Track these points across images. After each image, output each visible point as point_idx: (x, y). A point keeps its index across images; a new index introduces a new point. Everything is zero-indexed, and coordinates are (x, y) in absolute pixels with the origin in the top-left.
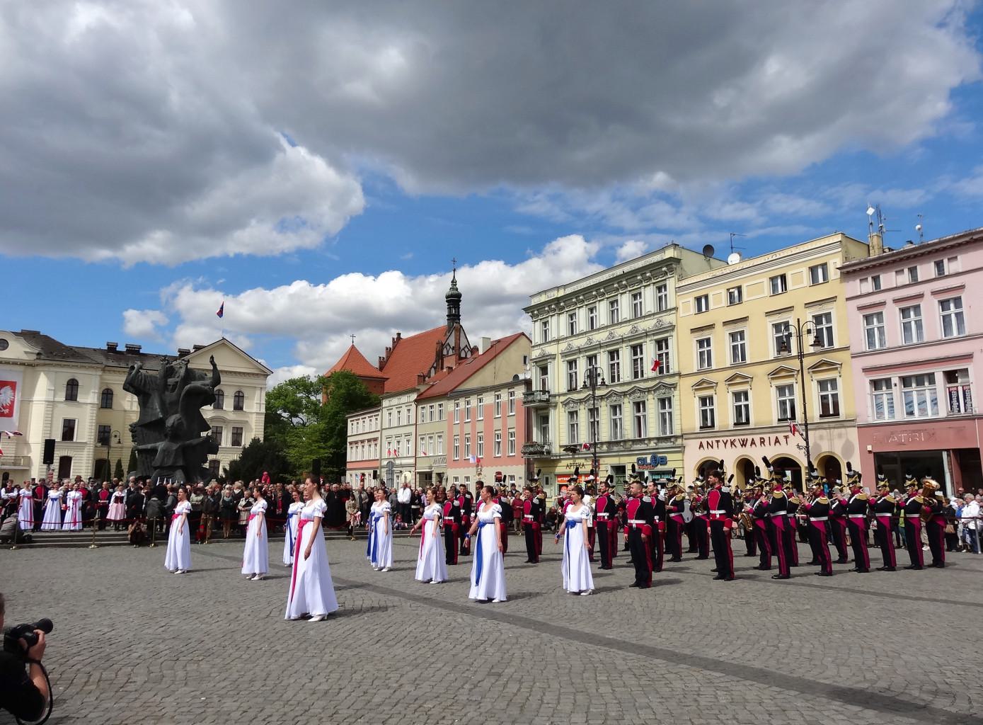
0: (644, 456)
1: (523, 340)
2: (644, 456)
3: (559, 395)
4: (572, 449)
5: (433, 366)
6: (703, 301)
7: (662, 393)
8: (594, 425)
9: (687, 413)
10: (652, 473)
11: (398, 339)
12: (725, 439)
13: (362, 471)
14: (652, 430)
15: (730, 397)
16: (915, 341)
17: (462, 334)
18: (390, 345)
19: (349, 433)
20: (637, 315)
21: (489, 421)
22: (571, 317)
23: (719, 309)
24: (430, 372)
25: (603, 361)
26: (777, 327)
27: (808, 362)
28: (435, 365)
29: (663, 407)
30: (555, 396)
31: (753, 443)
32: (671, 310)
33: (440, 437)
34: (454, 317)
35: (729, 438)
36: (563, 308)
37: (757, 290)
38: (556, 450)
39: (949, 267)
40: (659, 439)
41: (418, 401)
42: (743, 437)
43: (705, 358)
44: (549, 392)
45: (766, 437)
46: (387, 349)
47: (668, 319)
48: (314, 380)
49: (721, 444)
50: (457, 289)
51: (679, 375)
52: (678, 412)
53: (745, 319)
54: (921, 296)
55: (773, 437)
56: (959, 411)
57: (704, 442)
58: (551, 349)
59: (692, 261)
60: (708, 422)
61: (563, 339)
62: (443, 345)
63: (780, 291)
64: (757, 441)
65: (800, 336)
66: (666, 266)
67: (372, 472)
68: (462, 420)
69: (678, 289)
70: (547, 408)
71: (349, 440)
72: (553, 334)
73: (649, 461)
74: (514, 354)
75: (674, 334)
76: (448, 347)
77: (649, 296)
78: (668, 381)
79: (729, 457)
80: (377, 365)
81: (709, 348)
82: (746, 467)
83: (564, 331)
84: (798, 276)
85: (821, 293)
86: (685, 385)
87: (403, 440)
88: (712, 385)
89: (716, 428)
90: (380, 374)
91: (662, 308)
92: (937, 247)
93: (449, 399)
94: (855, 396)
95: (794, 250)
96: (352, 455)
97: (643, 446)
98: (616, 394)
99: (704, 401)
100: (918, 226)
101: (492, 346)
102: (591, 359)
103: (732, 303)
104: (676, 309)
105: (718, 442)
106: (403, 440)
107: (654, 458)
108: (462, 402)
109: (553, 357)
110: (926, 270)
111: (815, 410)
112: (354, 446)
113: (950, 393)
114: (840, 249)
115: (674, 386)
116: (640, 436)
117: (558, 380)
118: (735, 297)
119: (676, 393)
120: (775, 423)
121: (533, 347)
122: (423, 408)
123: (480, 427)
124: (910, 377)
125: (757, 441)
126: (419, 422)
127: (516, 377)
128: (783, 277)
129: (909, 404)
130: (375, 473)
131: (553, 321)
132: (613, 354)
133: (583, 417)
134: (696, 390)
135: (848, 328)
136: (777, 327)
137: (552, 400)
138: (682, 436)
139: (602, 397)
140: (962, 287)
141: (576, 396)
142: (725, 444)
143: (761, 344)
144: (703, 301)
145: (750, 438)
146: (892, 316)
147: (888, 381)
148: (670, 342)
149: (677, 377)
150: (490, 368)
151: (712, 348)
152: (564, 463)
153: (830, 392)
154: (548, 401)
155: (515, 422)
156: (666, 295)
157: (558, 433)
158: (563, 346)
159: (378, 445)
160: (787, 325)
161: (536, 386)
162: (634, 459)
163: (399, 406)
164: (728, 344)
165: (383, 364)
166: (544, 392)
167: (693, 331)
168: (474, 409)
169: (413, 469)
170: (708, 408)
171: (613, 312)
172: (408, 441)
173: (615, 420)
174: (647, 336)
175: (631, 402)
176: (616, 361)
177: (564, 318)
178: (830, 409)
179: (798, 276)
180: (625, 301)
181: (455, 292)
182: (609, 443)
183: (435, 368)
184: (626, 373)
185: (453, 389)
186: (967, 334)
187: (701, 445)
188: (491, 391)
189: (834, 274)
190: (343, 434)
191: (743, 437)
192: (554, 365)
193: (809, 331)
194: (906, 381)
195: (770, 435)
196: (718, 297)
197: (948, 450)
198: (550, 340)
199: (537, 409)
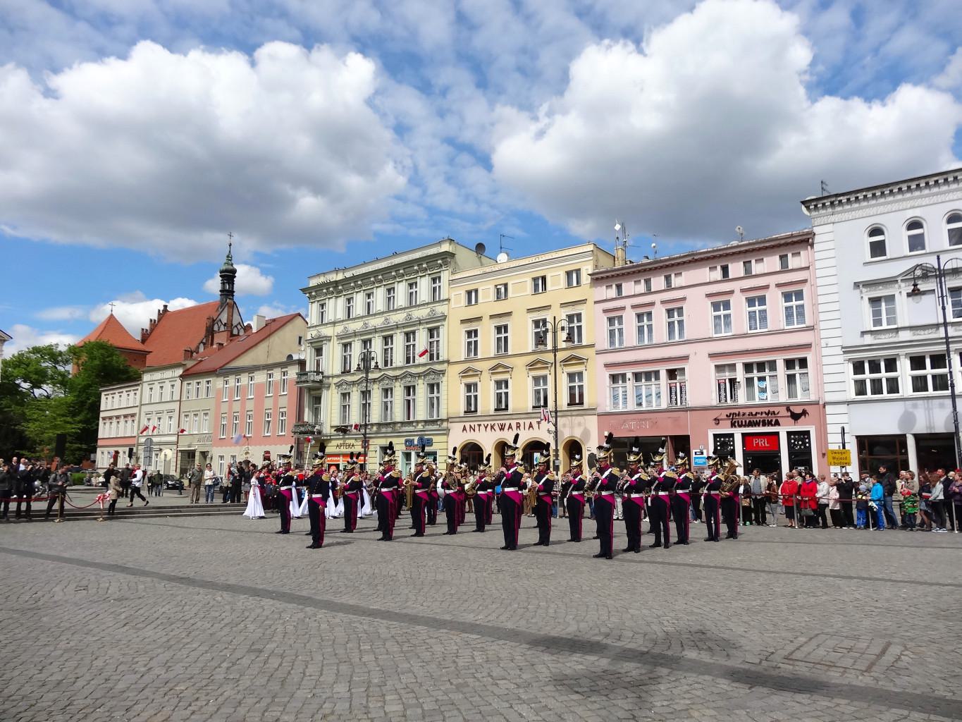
1: (299, 321)
3: (333, 377)
4: (343, 430)
6: (473, 294)
7: (430, 379)
8: (365, 407)
9: (453, 397)
11: (164, 313)
12: (486, 423)
13: (116, 449)
14: (421, 413)
15: (492, 385)
16: (646, 342)
17: (235, 310)
18: (155, 317)
20: (412, 303)
21: (260, 399)
22: (349, 300)
23: (487, 304)
24: (198, 347)
25: (377, 346)
26: (537, 323)
27: (561, 356)
29: (432, 392)
30: (328, 377)
31: (510, 427)
32: (443, 301)
33: (206, 414)
35: (489, 423)
36: (341, 291)
37: (520, 287)
38: (327, 430)
39: (676, 282)
40: (426, 422)
41: (183, 377)
42: (502, 422)
43: (472, 347)
44: (322, 373)
45: (521, 422)
46: (151, 320)
47: (440, 309)
48: (63, 348)
49: (482, 428)
50: (232, 265)
51: (448, 362)
53: (509, 314)
54: (652, 304)
55: (527, 422)
56: (676, 404)
57: (467, 425)
58: (327, 331)
59: (465, 256)
60: (471, 410)
61: (339, 322)
62: (214, 321)
63: (540, 291)
65: (555, 333)
66: (442, 259)
67: (127, 449)
68: (231, 397)
69: (452, 282)
70: (319, 389)
71: (102, 415)
72: (329, 317)
73: (416, 442)
74: (289, 333)
75: (445, 323)
76: (219, 323)
78: (438, 367)
80: (139, 338)
81: (506, 335)
83: (341, 315)
84: (556, 279)
85: (574, 295)
86: (453, 371)
87: (165, 417)
88: (477, 373)
89: (479, 413)
90: (141, 347)
91: (435, 297)
92: (667, 263)
93: (218, 376)
94: (597, 390)
95: (555, 255)
96: (104, 431)
97: (411, 428)
98: (388, 377)
99: (469, 387)
100: (653, 245)
101: (266, 325)
102: (366, 343)
103: (498, 298)
104: (448, 300)
105: (479, 425)
106: (165, 417)
107: (421, 439)
108: (232, 380)
109: (329, 339)
110: (658, 282)
111: (564, 399)
112: (108, 421)
113: (671, 388)
114: (591, 258)
115: (443, 372)
116: (409, 418)
117: (332, 362)
118: (501, 293)
119: (444, 379)
120: (530, 410)
121: (310, 327)
122: (189, 384)
123: (250, 405)
124: (641, 373)
126: (184, 398)
127: (290, 357)
128: (544, 278)
129: (639, 396)
130: (131, 450)
131: (330, 304)
132: (387, 339)
133: (355, 399)
134: (462, 377)
135: (594, 328)
136: (537, 323)
137: (326, 381)
138: (447, 420)
139: (374, 380)
140: (684, 299)
141: (349, 378)
142: (486, 428)
143: (522, 337)
144: (473, 294)
145: (507, 423)
146: (630, 318)
147: (624, 376)
148: (441, 330)
149: (446, 365)
150: (262, 348)
151: (479, 338)
152: (334, 443)
153: (577, 384)
154: (321, 381)
155: (286, 401)
156: (440, 287)
157: (330, 413)
158: (339, 329)
159: (136, 422)
160: (545, 322)
161: (309, 367)
162: (403, 440)
163: (162, 381)
164: (493, 335)
165: (146, 336)
166: (318, 372)
167: (463, 321)
168: (244, 386)
169: (175, 447)
170: (472, 394)
171: (389, 298)
172: (170, 418)
173: (386, 403)
174: (420, 324)
175: (402, 386)
176: (390, 346)
177: (341, 301)
178: (576, 399)
179: (556, 279)
181: (230, 267)
182: (379, 425)
183: (204, 344)
184: (398, 358)
185: (224, 365)
186: (685, 339)
187: (464, 429)
188: (264, 369)
189: (586, 279)
190: (95, 408)
191: (502, 422)
192: (329, 347)
193: (563, 329)
194: (637, 376)
195: (523, 421)
196: (487, 292)
198: (354, 316)
199: (310, 389)
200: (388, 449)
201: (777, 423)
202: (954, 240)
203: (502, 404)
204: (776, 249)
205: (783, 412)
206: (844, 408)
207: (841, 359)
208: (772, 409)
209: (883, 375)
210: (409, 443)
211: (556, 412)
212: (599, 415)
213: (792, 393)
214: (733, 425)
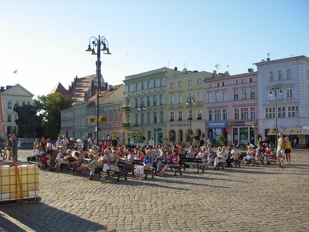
3: (133, 109)
4: (136, 126)
5: (90, 90)
11: (77, 80)
19: (62, 117)
24: (89, 92)
28: (91, 90)
31: (182, 125)
34: (99, 71)
46: (72, 82)
48: (46, 96)
52: (165, 116)
64: (183, 125)
71: (61, 119)
75: (165, 93)
77: (158, 81)
79: (176, 129)
82: (181, 132)
83: (135, 89)
96: (63, 125)
107: (158, 129)
125: (183, 125)
139: (145, 110)
142: (176, 125)
180: (152, 82)
187: (170, 126)
190: (59, 117)
200: (150, 132)
204: (249, 76)
206: (262, 121)
207: (262, 108)
210: (155, 130)
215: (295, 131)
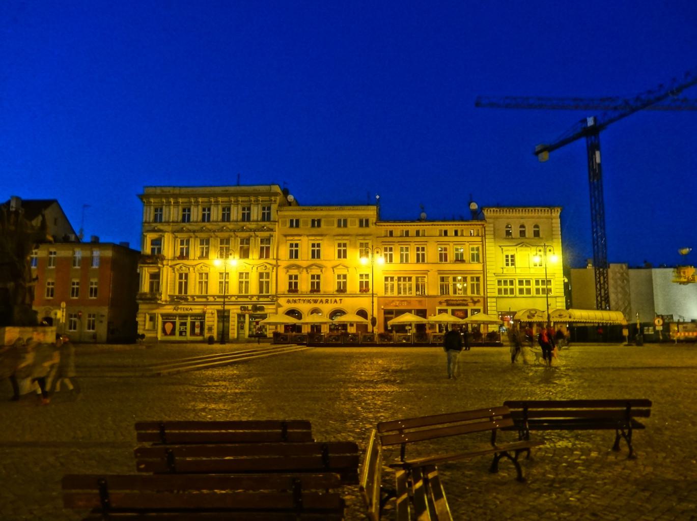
0: (246, 306)
2: (246, 306)
10: (251, 316)
12: (304, 298)
31: (321, 301)
35: (307, 298)
42: (317, 298)
55: (333, 299)
57: (291, 299)
60: (293, 288)
64: (324, 301)
116: (202, 293)
125: (324, 301)
129: (399, 289)
145: (320, 299)
162: (239, 307)
195: (332, 298)
197: (414, 310)
201: (467, 305)
202: (523, 235)
203: (315, 289)
205: (470, 300)
206: (494, 300)
208: (465, 299)
209: (509, 287)
210: (244, 308)
211: (373, 294)
212: (378, 297)
213: (473, 292)
214: (448, 305)
215: (566, 316)
